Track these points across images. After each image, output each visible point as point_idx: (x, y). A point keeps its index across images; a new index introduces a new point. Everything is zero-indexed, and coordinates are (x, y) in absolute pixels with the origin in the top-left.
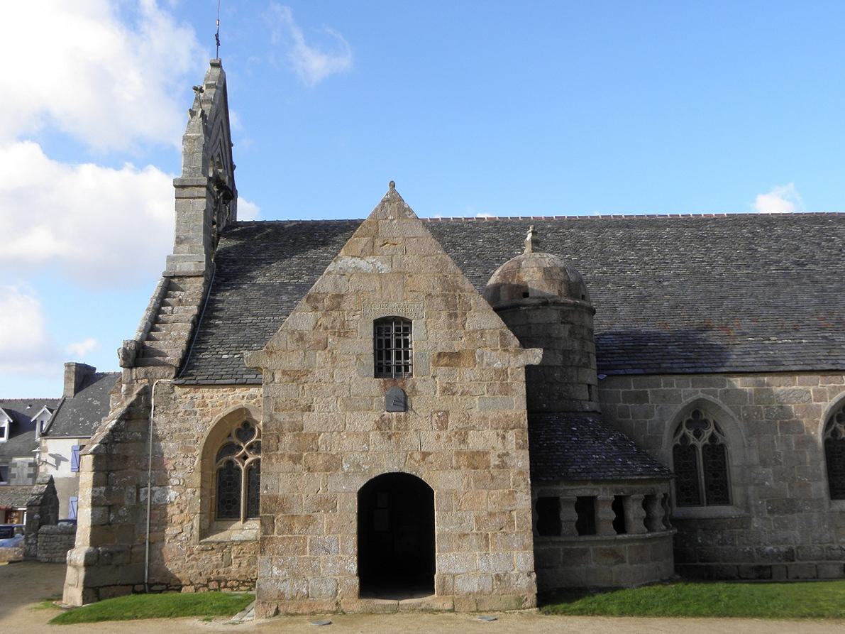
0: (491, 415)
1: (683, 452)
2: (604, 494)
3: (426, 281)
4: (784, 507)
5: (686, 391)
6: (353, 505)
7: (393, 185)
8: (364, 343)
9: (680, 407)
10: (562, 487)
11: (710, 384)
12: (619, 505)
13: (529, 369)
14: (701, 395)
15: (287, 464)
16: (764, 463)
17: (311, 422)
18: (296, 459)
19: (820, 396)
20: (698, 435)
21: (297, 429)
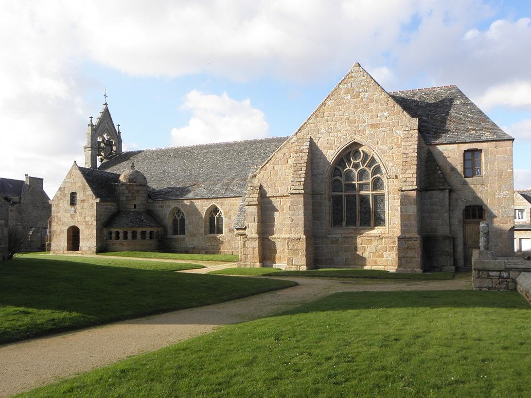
0: (90, 213)
1: (175, 221)
2: (121, 231)
3: (79, 184)
4: (194, 235)
5: (173, 205)
6: (66, 232)
7: (75, 162)
8: (68, 198)
9: (171, 209)
10: (112, 229)
11: (178, 202)
12: (126, 233)
13: (97, 203)
14: (176, 206)
15: (56, 224)
16: (189, 224)
17: (59, 215)
18: (57, 223)
19: (205, 205)
20: (179, 216)
21: (57, 216)
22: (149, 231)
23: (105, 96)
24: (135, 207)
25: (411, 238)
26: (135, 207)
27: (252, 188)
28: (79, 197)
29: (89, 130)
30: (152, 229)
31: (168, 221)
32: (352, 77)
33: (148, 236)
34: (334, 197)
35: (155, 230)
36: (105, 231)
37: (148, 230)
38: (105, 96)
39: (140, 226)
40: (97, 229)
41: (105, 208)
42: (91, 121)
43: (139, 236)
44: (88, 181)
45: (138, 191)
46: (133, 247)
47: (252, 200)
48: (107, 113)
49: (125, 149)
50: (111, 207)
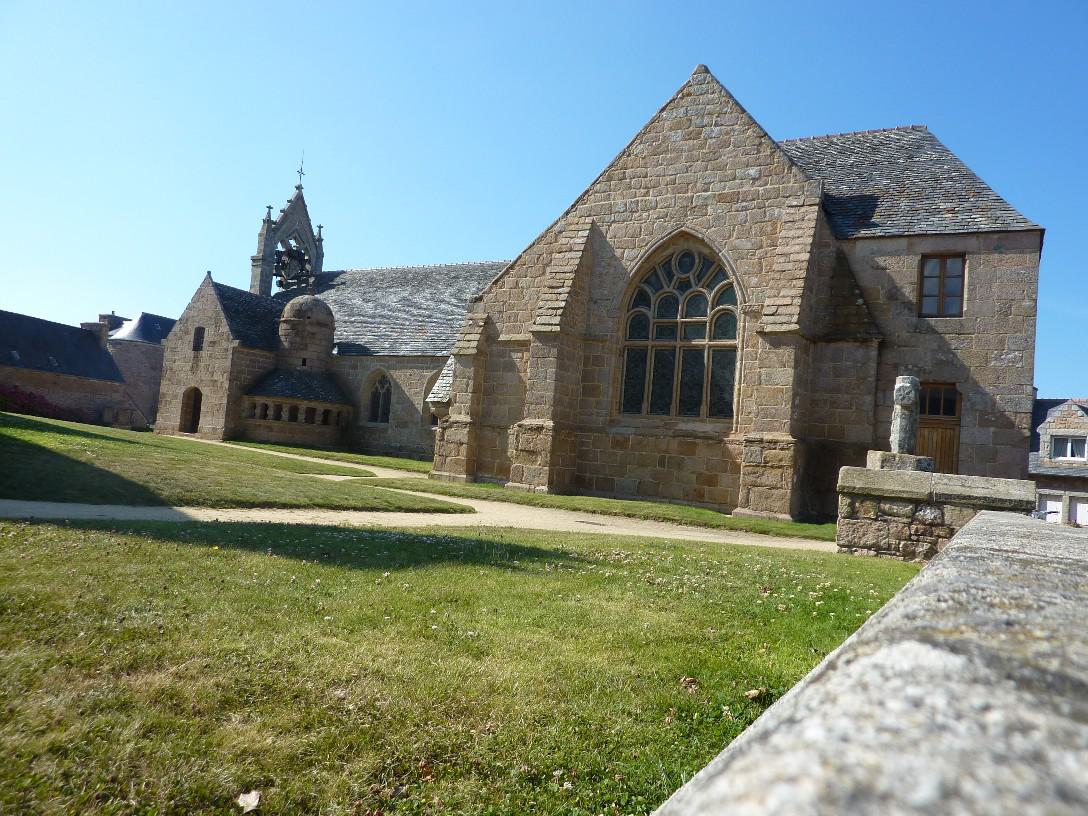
1: (375, 396)
4: (403, 424)
7: (209, 273)
8: (191, 337)
12: (279, 409)
18: (170, 380)
22: (322, 409)
23: (301, 172)
24: (304, 363)
25: (776, 442)
26: (304, 363)
27: (471, 322)
28: (208, 337)
29: (258, 227)
30: (328, 406)
31: (364, 397)
32: (689, 95)
33: (319, 418)
34: (631, 350)
35: (334, 408)
36: (246, 401)
37: (320, 407)
38: (301, 172)
39: (305, 398)
40: (228, 395)
41: (251, 360)
42: (269, 213)
43: (301, 417)
44: (226, 309)
45: (313, 334)
46: (287, 434)
47: (466, 344)
48: (300, 202)
49: (327, 266)
50: (262, 358)
